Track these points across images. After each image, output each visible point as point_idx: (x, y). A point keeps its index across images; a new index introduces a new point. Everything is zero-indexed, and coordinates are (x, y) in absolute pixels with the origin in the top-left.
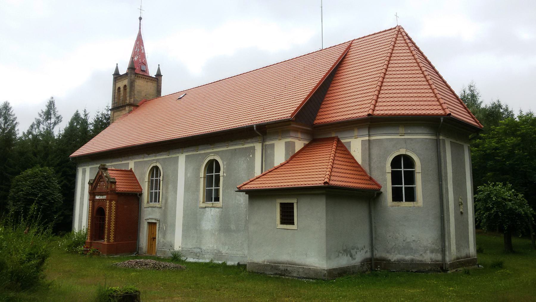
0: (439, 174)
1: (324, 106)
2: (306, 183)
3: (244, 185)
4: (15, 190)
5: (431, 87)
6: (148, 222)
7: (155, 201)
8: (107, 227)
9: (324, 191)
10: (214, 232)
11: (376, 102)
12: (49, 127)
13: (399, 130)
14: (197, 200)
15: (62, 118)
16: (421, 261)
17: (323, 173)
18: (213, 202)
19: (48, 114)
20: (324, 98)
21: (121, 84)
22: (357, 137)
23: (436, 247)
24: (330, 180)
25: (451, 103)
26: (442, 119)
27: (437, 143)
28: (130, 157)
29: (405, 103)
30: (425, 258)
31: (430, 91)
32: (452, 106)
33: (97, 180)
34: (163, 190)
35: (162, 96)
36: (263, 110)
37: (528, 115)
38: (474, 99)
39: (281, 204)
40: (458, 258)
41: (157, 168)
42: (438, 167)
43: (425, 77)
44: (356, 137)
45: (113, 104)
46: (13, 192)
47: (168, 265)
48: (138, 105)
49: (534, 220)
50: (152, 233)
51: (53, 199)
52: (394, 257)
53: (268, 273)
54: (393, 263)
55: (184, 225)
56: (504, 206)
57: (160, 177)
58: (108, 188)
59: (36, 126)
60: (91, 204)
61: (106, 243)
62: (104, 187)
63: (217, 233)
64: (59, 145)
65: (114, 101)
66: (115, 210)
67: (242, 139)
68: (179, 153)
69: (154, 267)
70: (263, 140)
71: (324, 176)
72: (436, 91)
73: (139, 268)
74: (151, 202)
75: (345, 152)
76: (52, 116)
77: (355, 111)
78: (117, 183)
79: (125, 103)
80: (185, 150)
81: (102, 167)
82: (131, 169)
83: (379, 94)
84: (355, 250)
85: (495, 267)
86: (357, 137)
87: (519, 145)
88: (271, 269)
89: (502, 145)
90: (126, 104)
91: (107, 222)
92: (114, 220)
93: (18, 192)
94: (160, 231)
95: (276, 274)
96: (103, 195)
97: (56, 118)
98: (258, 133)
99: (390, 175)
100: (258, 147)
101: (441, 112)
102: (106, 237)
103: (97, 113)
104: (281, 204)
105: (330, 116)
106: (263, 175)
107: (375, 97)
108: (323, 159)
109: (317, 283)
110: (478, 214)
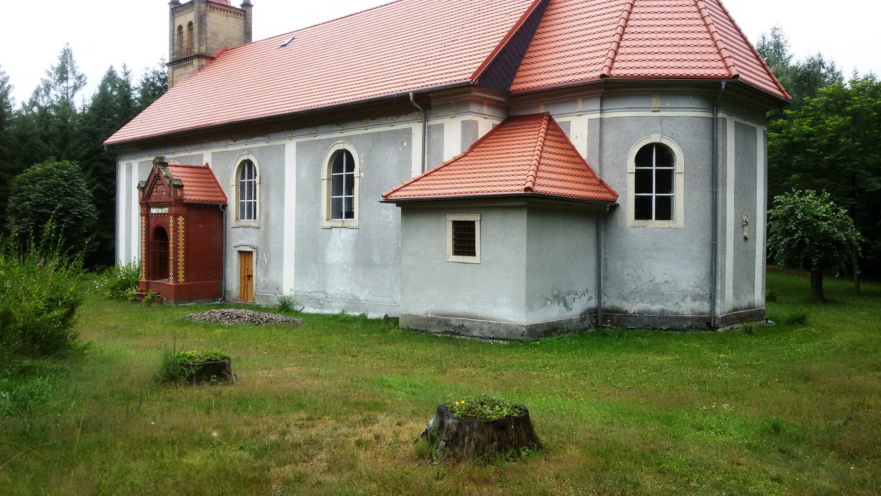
0: (713, 176)
1: (528, 61)
2: (495, 189)
3: (395, 191)
4: (16, 198)
5: (708, 28)
7: (249, 217)
8: (171, 258)
9: (523, 203)
10: (345, 267)
11: (616, 54)
12: (64, 94)
13: (651, 101)
14: (318, 215)
15: (86, 78)
16: (677, 313)
17: (524, 172)
18: (344, 219)
19: (62, 73)
20: (528, 47)
21: (183, 20)
22: (581, 114)
23: (701, 293)
24: (534, 184)
25: (741, 56)
26: (724, 84)
27: (714, 126)
28: (205, 145)
29: (664, 57)
30: (683, 309)
31: (708, 36)
32: (742, 62)
33: (152, 183)
35: (253, 40)
36: (426, 68)
37: (867, 79)
38: (779, 51)
39: (454, 222)
40: (735, 310)
41: (249, 163)
42: (713, 165)
43: (700, 11)
44: (579, 114)
45: (172, 54)
46: (14, 201)
47: (274, 319)
48: (213, 56)
49: (860, 251)
50: (246, 267)
51: (81, 214)
52: (632, 307)
53: (432, 330)
54: (631, 316)
55: (297, 256)
56: (814, 228)
57: (255, 178)
58: (170, 195)
59: (43, 92)
60: (144, 221)
61: (171, 283)
62: (164, 193)
63: (350, 269)
64: (85, 124)
65: (173, 49)
66: (183, 231)
68: (285, 138)
69: (252, 321)
70: (426, 118)
71: (525, 177)
72: (717, 37)
73: (226, 322)
74: (243, 218)
75: (561, 139)
76: (70, 75)
77: (580, 70)
78: (185, 188)
79: (191, 53)
81: (158, 161)
82: (207, 164)
83: (621, 40)
84: (573, 296)
85: (793, 323)
86: (581, 114)
87: (848, 128)
88: (438, 324)
89: (820, 129)
90: (193, 55)
91: (171, 250)
92: (183, 248)
93: (23, 201)
94: (258, 264)
95: (446, 332)
96: (162, 207)
97: (77, 78)
98: (417, 106)
99: (633, 177)
100: (417, 129)
101: (724, 72)
102: (171, 274)
103: (145, 71)
104: (456, 224)
105: (537, 77)
106: (426, 176)
107: (614, 46)
108: (524, 150)
109: (511, 347)
110: (772, 241)
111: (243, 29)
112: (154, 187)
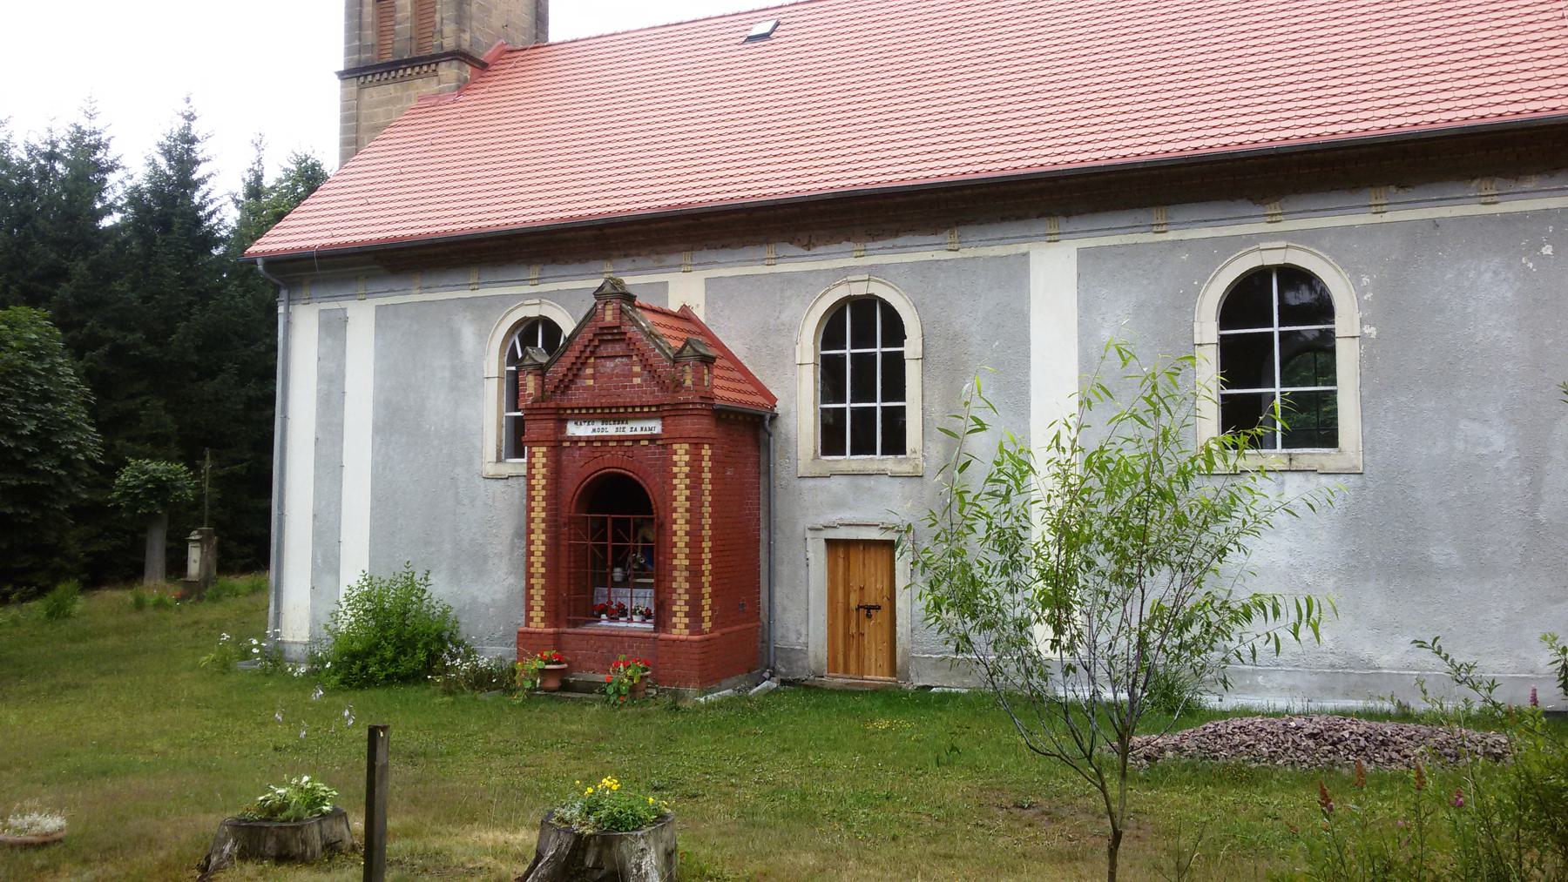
6: (827, 540)
7: (863, 446)
8: (681, 561)
28: (672, 259)
34: (927, 399)
35: (552, 38)
41: (864, 307)
45: (349, 51)
50: (854, 584)
67: (1473, 178)
80: (1076, 223)
111: (534, 11)
112: (584, 364)
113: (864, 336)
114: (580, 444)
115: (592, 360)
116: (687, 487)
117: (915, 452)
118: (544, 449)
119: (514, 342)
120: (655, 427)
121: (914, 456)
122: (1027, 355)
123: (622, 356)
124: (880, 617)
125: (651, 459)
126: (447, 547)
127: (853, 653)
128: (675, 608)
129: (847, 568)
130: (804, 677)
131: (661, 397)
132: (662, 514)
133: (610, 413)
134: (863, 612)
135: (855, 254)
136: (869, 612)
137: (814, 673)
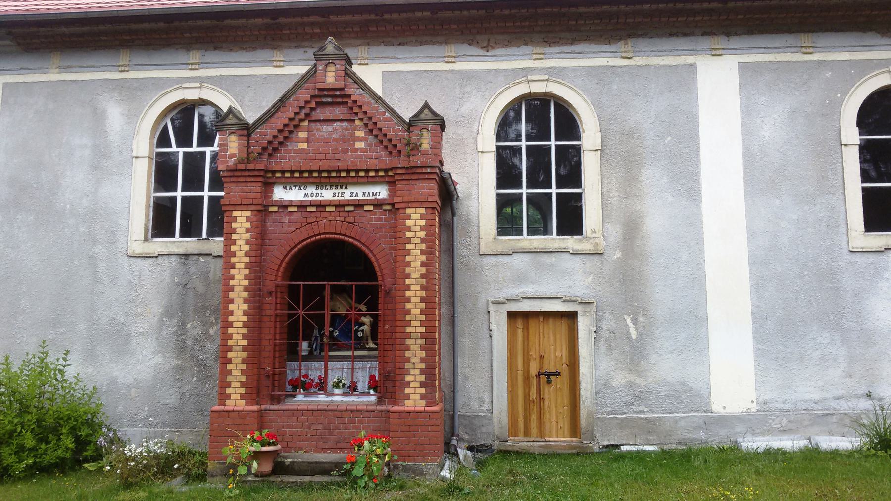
6: (508, 312)
7: (540, 227)
8: (416, 328)
34: (605, 185)
50: (534, 353)
55: (759, 317)
68: (694, 52)
94: (602, 343)
112: (296, 126)
113: (540, 131)
114: (290, 209)
115: (306, 123)
116: (422, 253)
117: (595, 232)
118: (249, 213)
119: (166, 124)
120: (382, 192)
121: (594, 235)
122: (697, 151)
123: (342, 120)
124: (561, 383)
125: (375, 225)
126: (82, 327)
127: (534, 417)
128: (408, 378)
129: (526, 338)
130: (488, 442)
131: (386, 160)
132: (389, 281)
133: (329, 177)
134: (544, 379)
135: (534, 57)
136: (549, 378)
137: (498, 438)
